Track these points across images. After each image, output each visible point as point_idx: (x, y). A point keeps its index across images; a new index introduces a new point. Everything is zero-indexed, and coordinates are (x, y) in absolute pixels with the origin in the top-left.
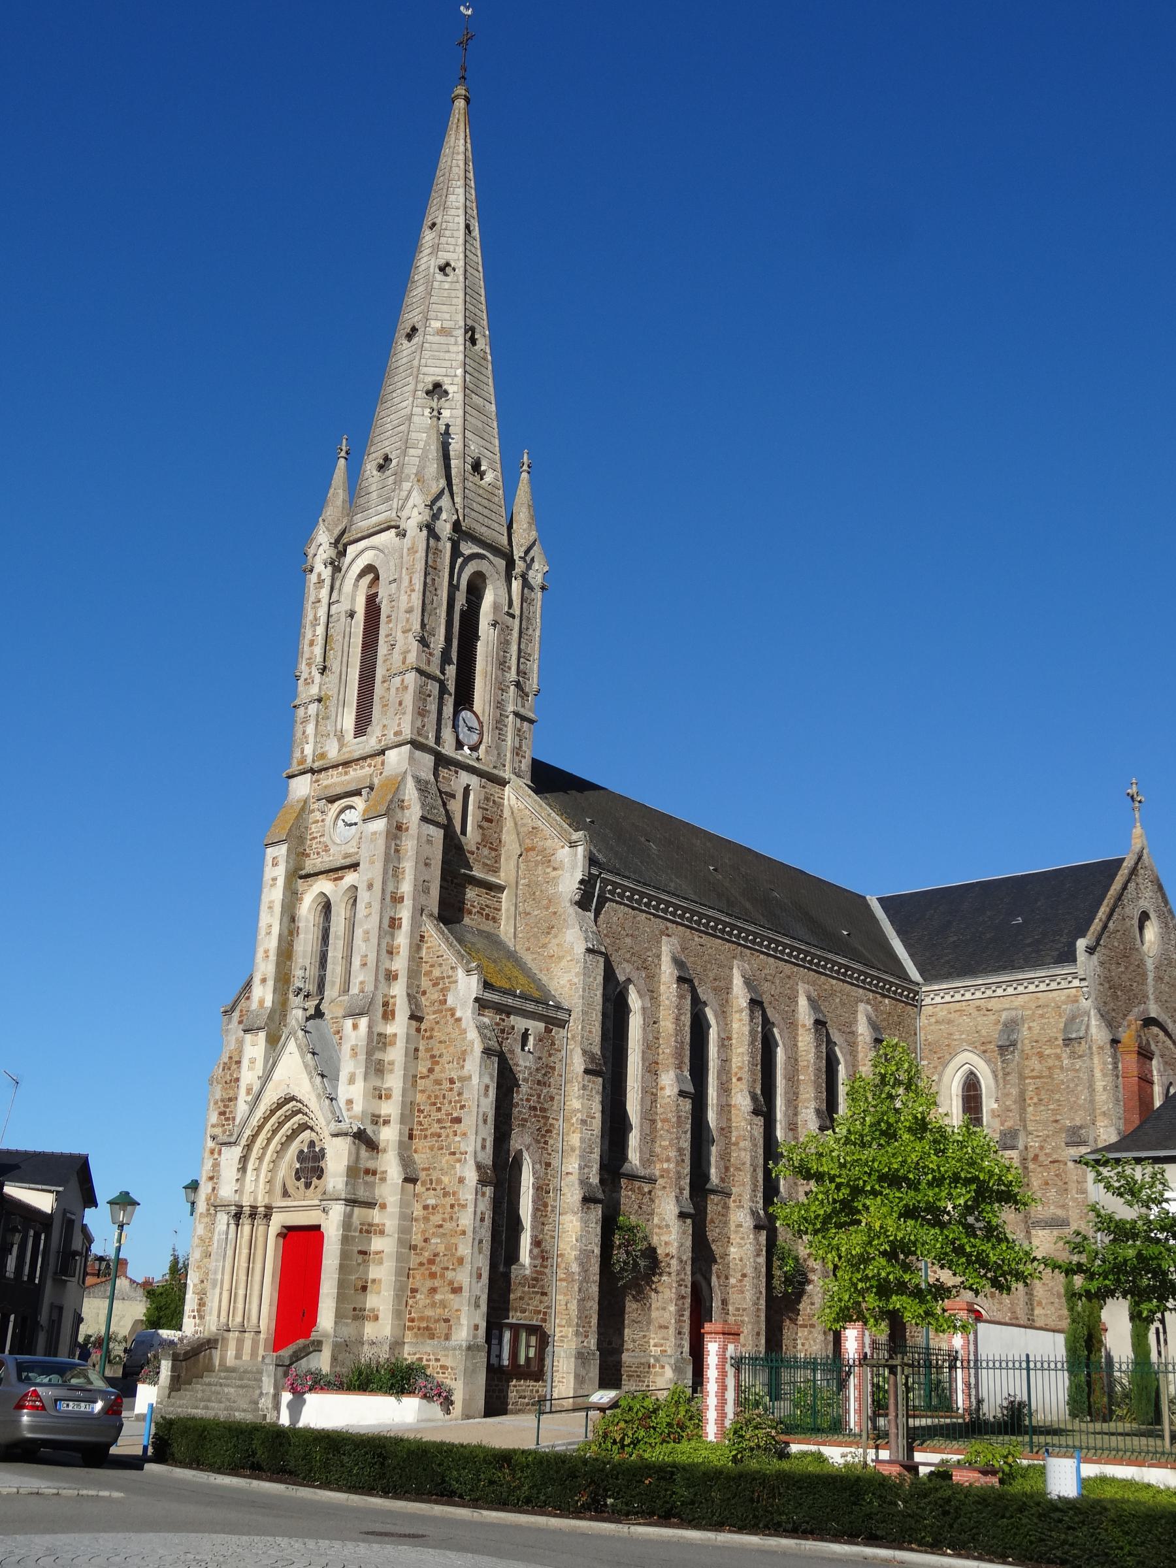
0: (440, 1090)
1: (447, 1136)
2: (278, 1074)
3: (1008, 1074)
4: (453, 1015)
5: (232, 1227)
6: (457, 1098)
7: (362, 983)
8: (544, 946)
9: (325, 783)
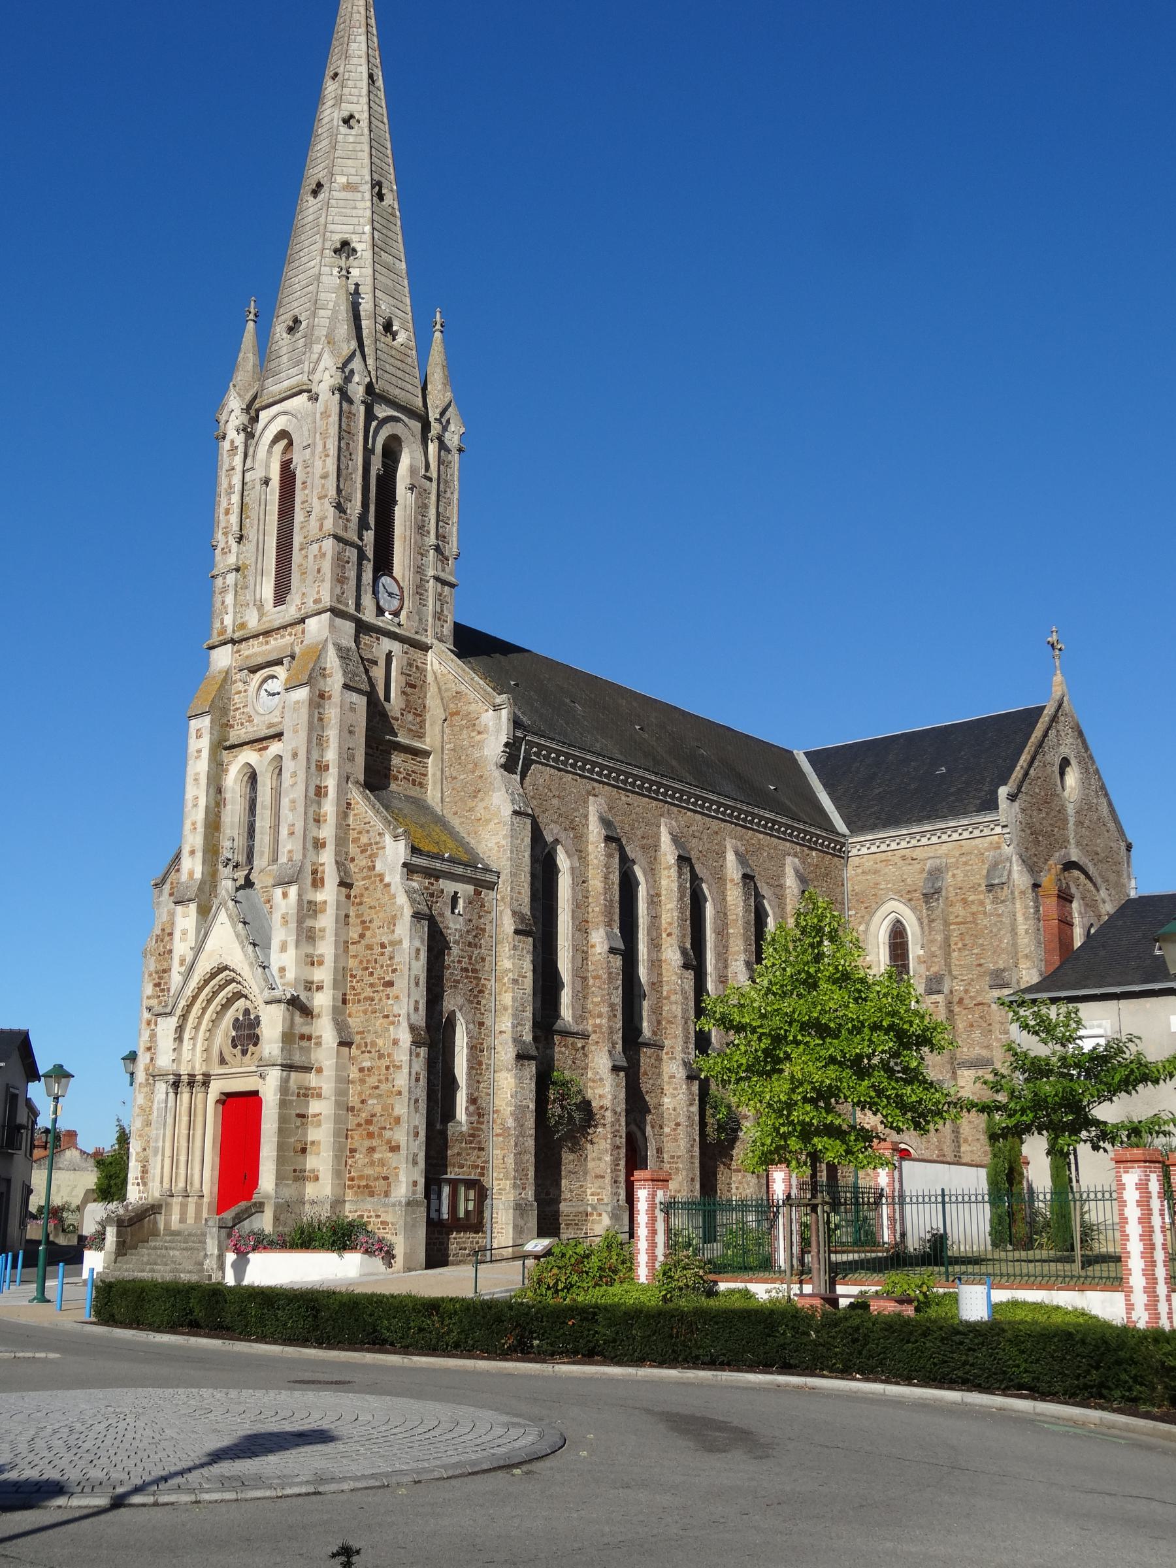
0: (372, 954)
1: (380, 1000)
2: (210, 945)
3: (933, 920)
4: (382, 880)
5: (171, 1096)
7: (290, 852)
8: (471, 810)
9: (247, 653)
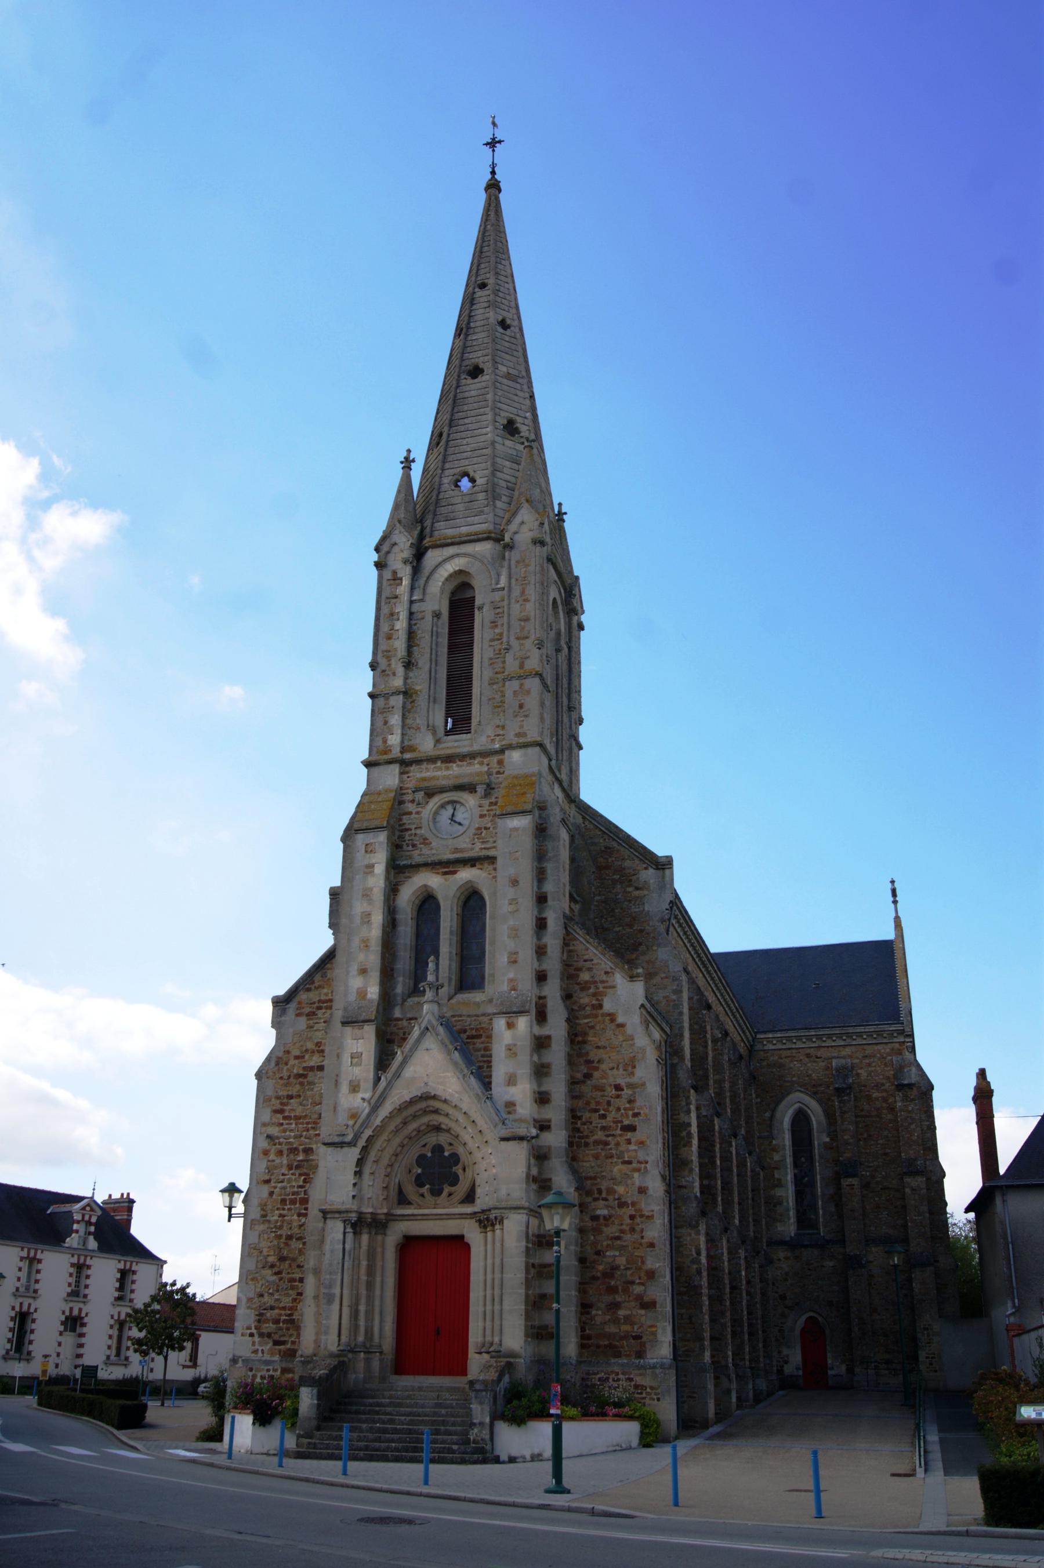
0: (603, 1096)
1: (618, 1144)
3: (845, 1112)
4: (612, 1020)
5: (350, 1237)
6: (628, 1105)
7: (511, 980)
9: (419, 775)
